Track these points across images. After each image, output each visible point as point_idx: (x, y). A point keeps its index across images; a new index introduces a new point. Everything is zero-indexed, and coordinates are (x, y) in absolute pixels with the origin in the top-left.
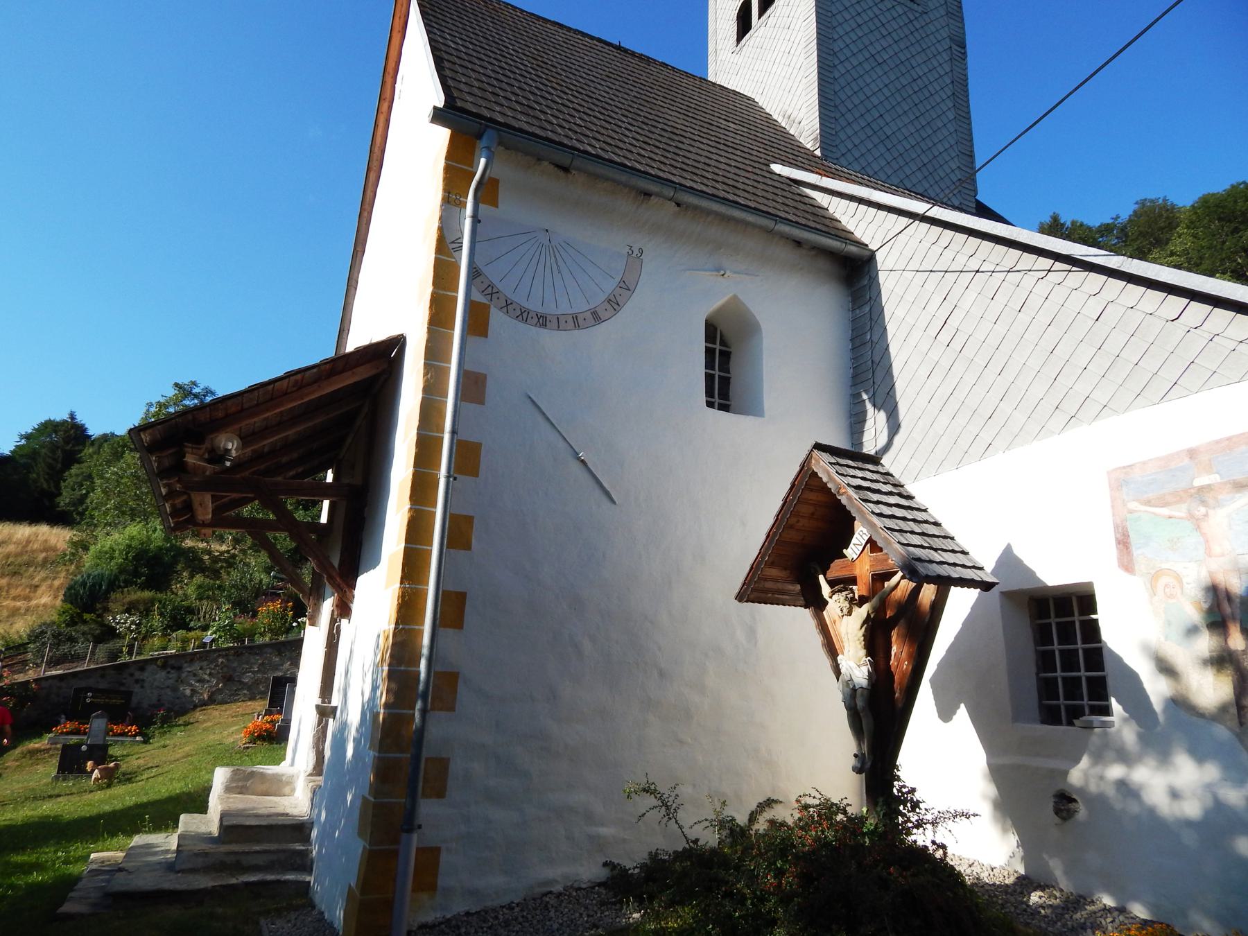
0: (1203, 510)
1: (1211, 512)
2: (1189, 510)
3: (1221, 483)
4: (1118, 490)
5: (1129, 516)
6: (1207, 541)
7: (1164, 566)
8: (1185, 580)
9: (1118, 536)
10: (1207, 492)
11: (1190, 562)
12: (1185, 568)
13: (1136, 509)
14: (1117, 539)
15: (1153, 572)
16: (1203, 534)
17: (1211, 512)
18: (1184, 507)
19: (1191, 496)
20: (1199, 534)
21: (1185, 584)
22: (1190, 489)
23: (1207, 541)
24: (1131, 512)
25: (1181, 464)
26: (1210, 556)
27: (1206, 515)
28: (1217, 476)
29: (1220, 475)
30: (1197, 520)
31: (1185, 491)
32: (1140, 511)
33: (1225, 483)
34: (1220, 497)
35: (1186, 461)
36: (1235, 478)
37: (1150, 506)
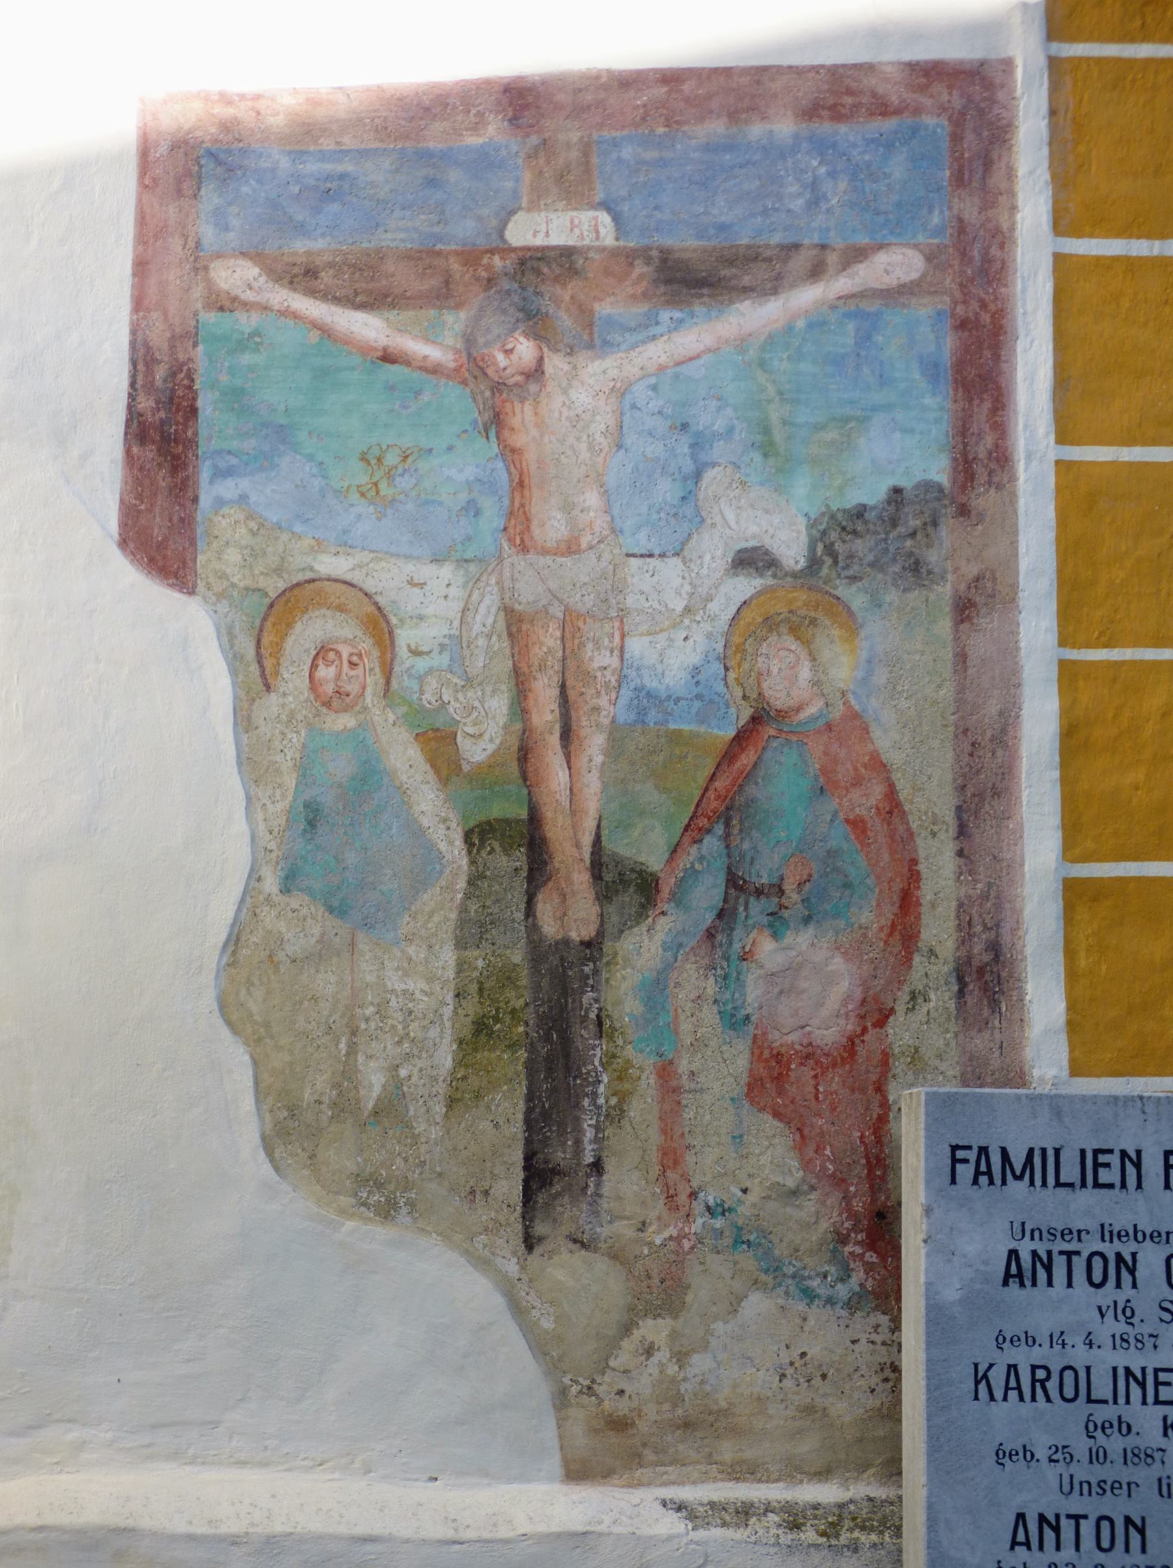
0: (525, 349)
1: (555, 364)
2: (469, 340)
3: (615, 253)
4: (179, 192)
5: (210, 318)
6: (520, 485)
7: (330, 565)
8: (405, 637)
9: (145, 403)
10: (556, 279)
11: (436, 560)
12: (411, 583)
13: (249, 296)
14: (133, 416)
15: (275, 586)
16: (511, 454)
17: (555, 364)
18: (455, 321)
19: (490, 282)
20: (495, 448)
21: (402, 652)
22: (492, 252)
23: (520, 485)
24: (225, 304)
25: (473, 140)
26: (524, 548)
27: (536, 373)
28: (605, 218)
29: (616, 218)
30: (498, 387)
31: (471, 257)
32: (266, 308)
33: (630, 256)
34: (605, 309)
35: (494, 130)
36: (668, 241)
37: (312, 293)
